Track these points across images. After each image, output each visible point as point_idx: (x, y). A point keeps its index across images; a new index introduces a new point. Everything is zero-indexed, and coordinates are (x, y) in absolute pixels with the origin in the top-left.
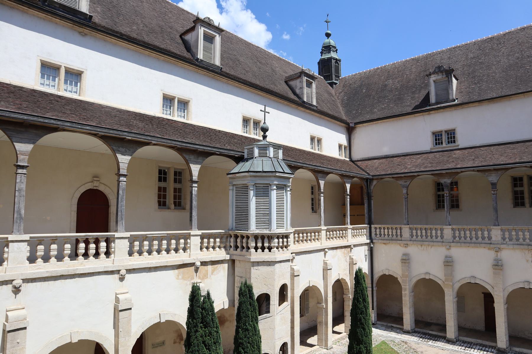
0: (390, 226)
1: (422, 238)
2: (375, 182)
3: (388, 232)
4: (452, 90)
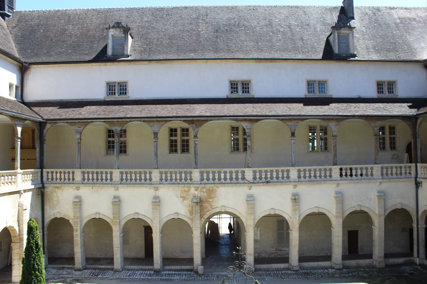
0: (62, 170)
1: (93, 181)
2: (48, 126)
3: (61, 176)
4: (127, 47)
